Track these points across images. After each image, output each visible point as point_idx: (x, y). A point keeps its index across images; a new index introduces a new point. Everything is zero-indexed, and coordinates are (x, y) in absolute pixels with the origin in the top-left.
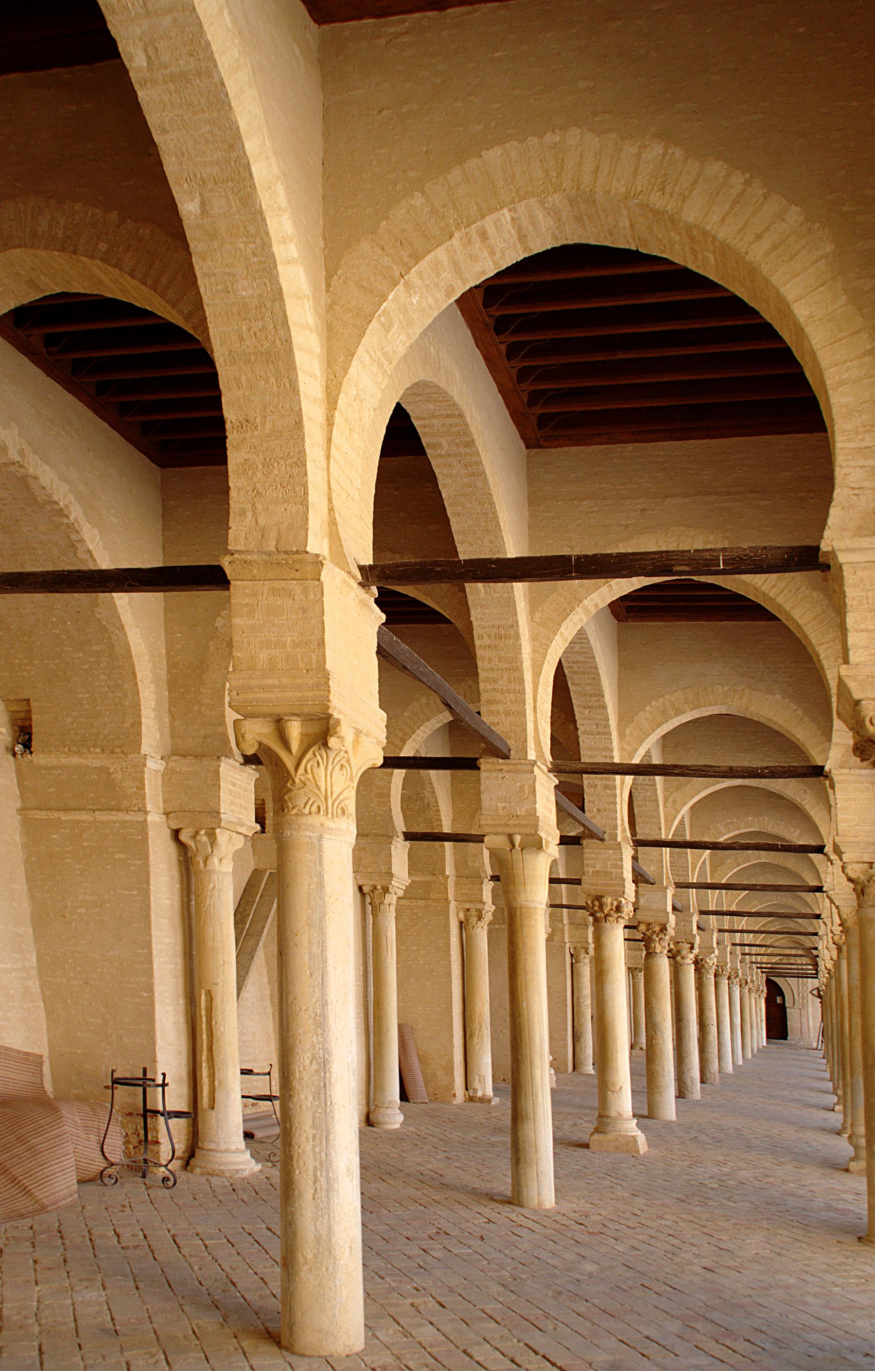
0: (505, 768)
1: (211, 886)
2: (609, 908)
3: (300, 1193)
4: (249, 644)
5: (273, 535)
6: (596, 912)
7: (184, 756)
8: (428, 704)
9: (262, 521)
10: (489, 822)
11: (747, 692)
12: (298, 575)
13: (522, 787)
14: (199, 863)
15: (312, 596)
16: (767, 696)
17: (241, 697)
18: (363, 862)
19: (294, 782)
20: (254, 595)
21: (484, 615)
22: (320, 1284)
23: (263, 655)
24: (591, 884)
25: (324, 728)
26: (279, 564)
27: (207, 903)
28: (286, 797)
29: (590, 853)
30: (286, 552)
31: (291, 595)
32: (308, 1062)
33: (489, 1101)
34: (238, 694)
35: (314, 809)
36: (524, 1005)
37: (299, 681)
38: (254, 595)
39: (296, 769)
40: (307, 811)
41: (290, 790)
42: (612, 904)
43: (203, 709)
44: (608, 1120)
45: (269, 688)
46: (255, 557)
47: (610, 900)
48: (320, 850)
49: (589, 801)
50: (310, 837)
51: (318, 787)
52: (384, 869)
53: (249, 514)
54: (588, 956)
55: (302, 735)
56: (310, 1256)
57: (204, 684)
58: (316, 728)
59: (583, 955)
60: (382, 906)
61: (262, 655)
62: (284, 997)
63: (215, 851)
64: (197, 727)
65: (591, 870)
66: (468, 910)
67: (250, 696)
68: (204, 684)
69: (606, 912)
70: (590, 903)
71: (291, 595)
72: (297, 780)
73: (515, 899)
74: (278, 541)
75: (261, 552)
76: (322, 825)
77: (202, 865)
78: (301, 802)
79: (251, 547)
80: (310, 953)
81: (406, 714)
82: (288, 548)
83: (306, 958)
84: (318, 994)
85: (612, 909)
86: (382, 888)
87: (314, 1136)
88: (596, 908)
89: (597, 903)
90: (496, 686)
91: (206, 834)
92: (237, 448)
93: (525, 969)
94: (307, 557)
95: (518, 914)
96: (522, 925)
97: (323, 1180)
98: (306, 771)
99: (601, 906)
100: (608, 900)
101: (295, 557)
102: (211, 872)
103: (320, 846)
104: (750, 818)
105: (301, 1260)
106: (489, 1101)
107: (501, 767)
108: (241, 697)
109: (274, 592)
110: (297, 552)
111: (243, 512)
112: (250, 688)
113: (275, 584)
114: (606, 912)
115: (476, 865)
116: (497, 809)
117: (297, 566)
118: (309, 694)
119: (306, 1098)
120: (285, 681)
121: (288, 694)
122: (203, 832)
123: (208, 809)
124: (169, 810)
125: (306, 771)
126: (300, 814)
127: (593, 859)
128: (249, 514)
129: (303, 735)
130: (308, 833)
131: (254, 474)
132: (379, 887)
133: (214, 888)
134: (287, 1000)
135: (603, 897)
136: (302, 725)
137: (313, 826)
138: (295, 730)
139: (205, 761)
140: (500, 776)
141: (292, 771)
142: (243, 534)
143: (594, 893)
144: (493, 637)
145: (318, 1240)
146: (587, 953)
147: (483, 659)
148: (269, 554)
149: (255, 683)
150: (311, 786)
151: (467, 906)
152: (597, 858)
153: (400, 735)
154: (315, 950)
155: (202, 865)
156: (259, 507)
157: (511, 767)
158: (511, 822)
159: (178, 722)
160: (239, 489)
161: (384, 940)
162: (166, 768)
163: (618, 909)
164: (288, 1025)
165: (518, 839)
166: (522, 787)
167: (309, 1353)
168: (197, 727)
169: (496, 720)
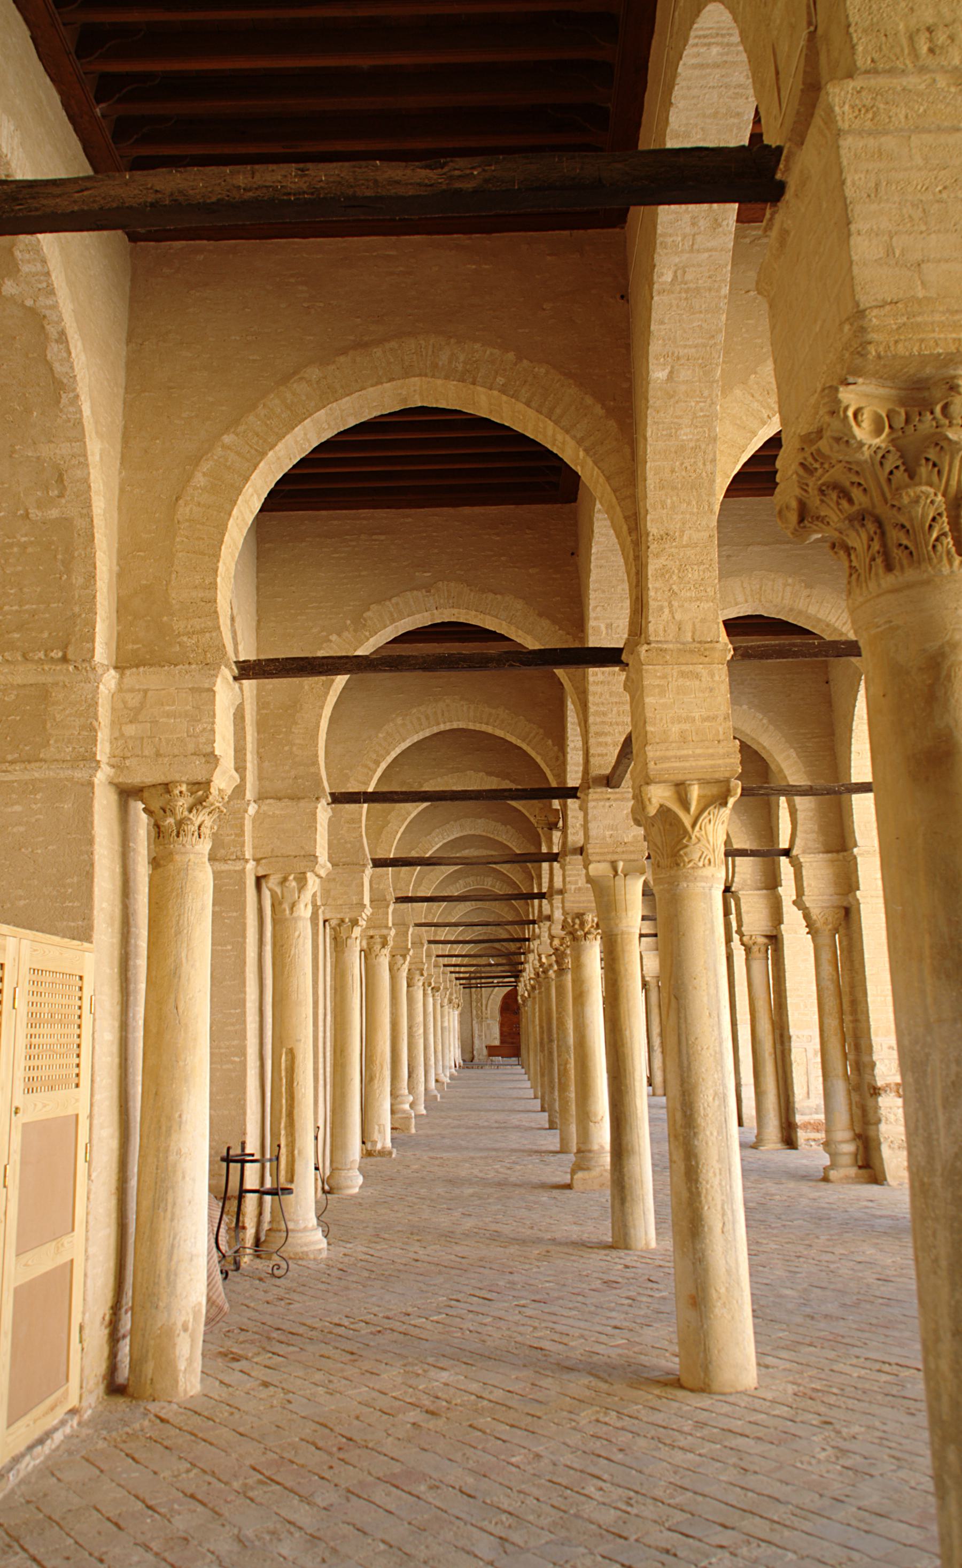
4: (661, 719)
5: (688, 628)
9: (678, 616)
15: (717, 678)
17: (659, 766)
19: (690, 838)
20: (664, 677)
22: (733, 1317)
23: (675, 729)
25: (724, 789)
26: (692, 651)
30: (700, 642)
31: (698, 676)
32: (711, 1099)
37: (711, 751)
39: (694, 826)
40: (701, 864)
41: (686, 846)
45: (680, 758)
46: (671, 646)
53: (666, 611)
56: (723, 1290)
58: (714, 790)
62: (683, 1039)
71: (698, 676)
74: (694, 633)
75: (677, 642)
78: (696, 856)
79: (670, 638)
80: (708, 994)
82: (703, 639)
83: (705, 999)
84: (716, 1033)
92: (657, 556)
94: (717, 645)
97: (729, 1212)
101: (707, 645)
105: (714, 1295)
108: (659, 766)
109: (683, 674)
111: (661, 609)
112: (667, 759)
113: (683, 668)
117: (707, 653)
120: (698, 751)
121: (702, 763)
126: (695, 868)
128: (666, 611)
130: (703, 884)
131: (671, 577)
134: (687, 1040)
138: (695, 792)
141: (689, 829)
145: (728, 1272)
149: (670, 753)
150: (704, 841)
156: (675, 604)
160: (657, 590)
164: (689, 1064)
167: (728, 1390)
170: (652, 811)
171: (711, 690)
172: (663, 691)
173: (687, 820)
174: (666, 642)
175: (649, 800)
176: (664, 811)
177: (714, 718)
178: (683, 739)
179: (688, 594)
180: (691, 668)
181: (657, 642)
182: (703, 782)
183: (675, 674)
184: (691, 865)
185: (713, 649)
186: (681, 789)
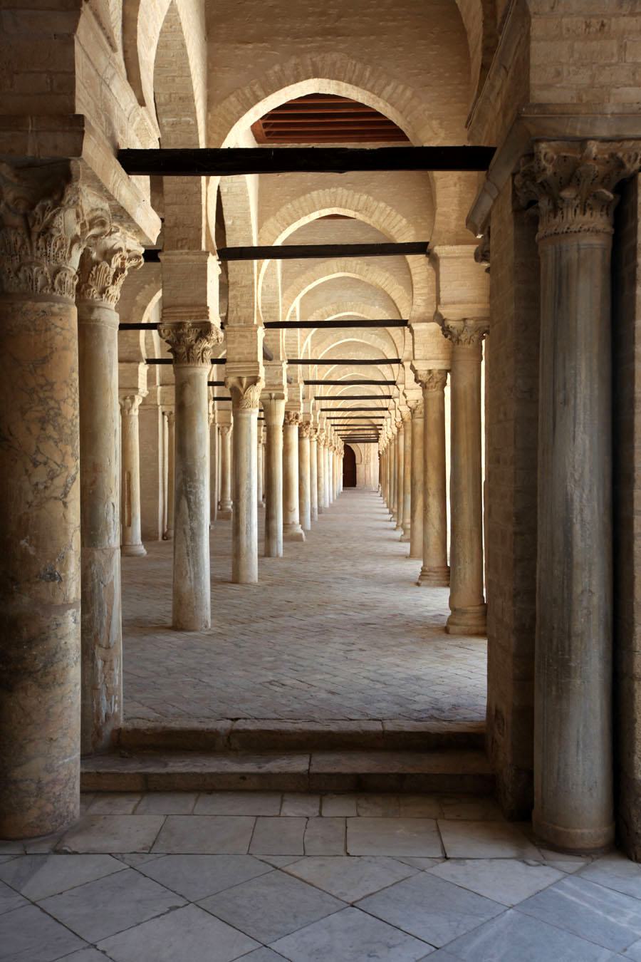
13: (277, 373)
31: (246, 337)
38: (234, 337)
53: (235, 312)
58: (252, 380)
71: (246, 337)
77: (127, 413)
83: (245, 455)
100: (292, 413)
102: (131, 416)
104: (352, 353)
109: (241, 336)
111: (233, 311)
126: (245, 408)
128: (235, 312)
129: (247, 382)
138: (245, 381)
139: (132, 365)
154: (248, 452)
155: (127, 413)
163: (297, 417)
165: (273, 395)
166: (277, 373)
173: (242, 391)
186: (240, 379)
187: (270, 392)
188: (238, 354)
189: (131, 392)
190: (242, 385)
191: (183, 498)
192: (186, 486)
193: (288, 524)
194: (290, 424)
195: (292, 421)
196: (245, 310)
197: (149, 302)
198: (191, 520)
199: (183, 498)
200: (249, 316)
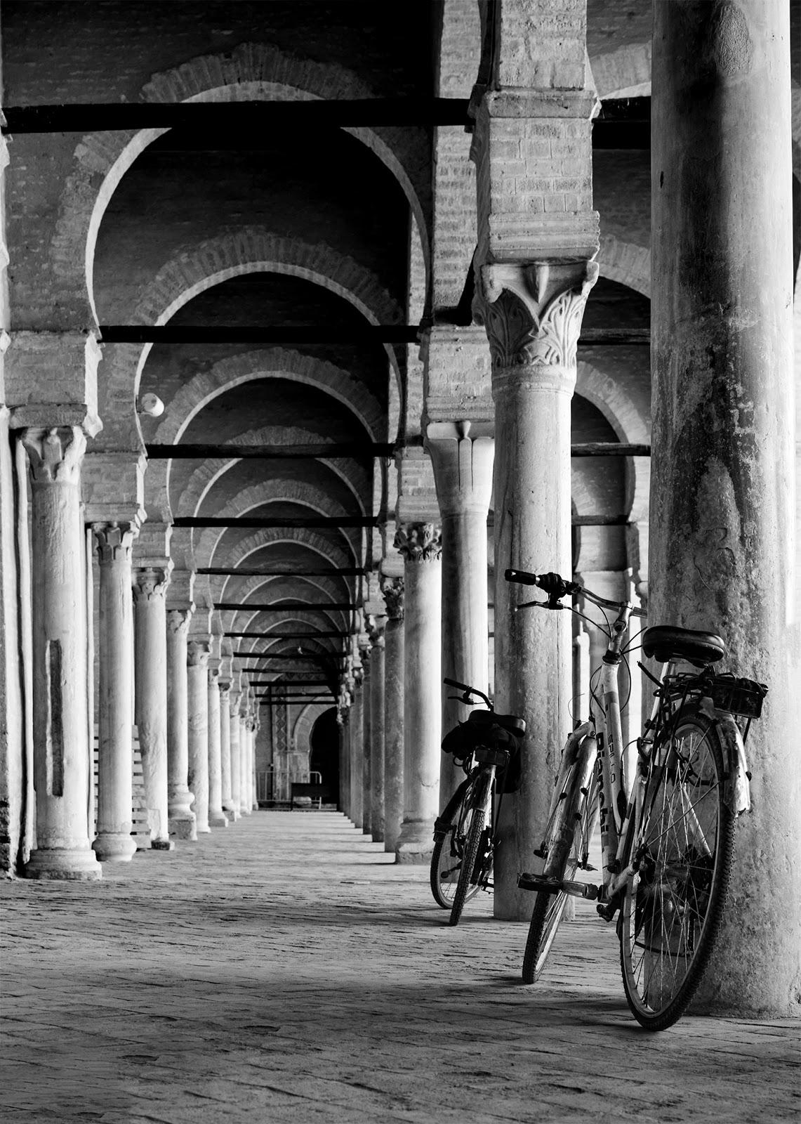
0: (460, 337)
1: (61, 503)
2: (431, 539)
3: (534, 758)
5: (546, 71)
6: (414, 546)
7: (38, 331)
8: (190, 264)
9: (536, 56)
10: (438, 406)
11: (615, 243)
12: (566, 112)
14: (46, 473)
15: (578, 135)
16: (641, 249)
18: (96, 488)
19: (537, 330)
20: (516, 132)
21: (454, 144)
23: (525, 197)
24: (410, 508)
25: (579, 272)
26: (549, 101)
27: (57, 526)
28: (526, 348)
29: (410, 465)
30: (560, 89)
31: (555, 133)
32: (543, 623)
33: (166, 846)
34: (500, 238)
35: (554, 359)
36: (467, 634)
37: (565, 224)
39: (541, 316)
40: (547, 361)
41: (532, 340)
42: (435, 534)
43: (55, 267)
44: (422, 825)
45: (528, 232)
46: (524, 94)
47: (432, 527)
48: (557, 403)
49: (413, 394)
50: (549, 389)
51: (558, 337)
52: (125, 497)
53: (522, 49)
54: (207, 654)
55: (550, 281)
57: (57, 234)
59: (200, 652)
60: (118, 552)
61: (523, 197)
63: (67, 457)
64: (46, 291)
65: (411, 488)
66: (143, 570)
67: (511, 240)
68: (57, 234)
69: (426, 545)
70: (405, 532)
71: (555, 133)
72: (540, 329)
73: (460, 503)
74: (553, 77)
75: (533, 88)
76: (561, 376)
77: (50, 475)
78: (541, 352)
79: (524, 83)
80: (547, 509)
81: (158, 278)
82: (564, 85)
83: (543, 515)
84: (554, 553)
85: (434, 541)
86: (120, 525)
87: (548, 698)
88: (414, 540)
89: (415, 533)
90: (456, 234)
91: (58, 433)
93: (469, 591)
94: (581, 94)
95: (462, 521)
96: (466, 535)
98: (549, 320)
99: (421, 537)
101: (568, 94)
102: (60, 485)
103: (557, 397)
106: (166, 846)
107: (456, 336)
108: (503, 241)
109: (538, 130)
110: (574, 89)
113: (540, 122)
114: (426, 545)
115: (156, 504)
116: (448, 391)
117: (568, 103)
118: (576, 237)
119: (541, 660)
120: (551, 224)
122: (54, 432)
123: (68, 400)
124: (13, 402)
125: (549, 320)
127: (414, 473)
128: (522, 49)
130: (548, 385)
131: (529, 5)
132: (115, 524)
133: (64, 506)
135: (424, 524)
136: (551, 271)
137: (554, 377)
138: (545, 276)
139: (67, 338)
140: (454, 346)
141: (537, 320)
142: (515, 69)
143: (414, 519)
144: (459, 173)
146: (207, 650)
147: (444, 199)
148: (541, 91)
149: (518, 226)
150: (552, 335)
151: (143, 564)
152: (419, 472)
153: (150, 307)
154: (552, 507)
155: (50, 475)
156: (533, 40)
157: (468, 336)
158: (466, 405)
159: (20, 286)
160: (511, 21)
161: (120, 598)
162: (10, 347)
165: (468, 427)
168: (46, 291)
169: (453, 278)
170: (494, 296)
171: (570, 150)
172: (513, 150)
173: (534, 309)
174: (519, 88)
175: (491, 282)
176: (507, 296)
177: (572, 185)
178: (534, 207)
179: (550, 28)
180: (548, 122)
181: (509, 87)
182: (554, 262)
183: (529, 129)
184: (535, 362)
185: (575, 99)
186: (527, 269)
187: (461, 415)
188: (531, 186)
189: (65, 416)
190: (532, 290)
191: (715, 464)
192: (725, 414)
193: (420, 821)
194: (425, 553)
195: (429, 549)
196: (554, 43)
197: (112, 163)
198: (749, 556)
199: (715, 464)
200: (566, 62)
